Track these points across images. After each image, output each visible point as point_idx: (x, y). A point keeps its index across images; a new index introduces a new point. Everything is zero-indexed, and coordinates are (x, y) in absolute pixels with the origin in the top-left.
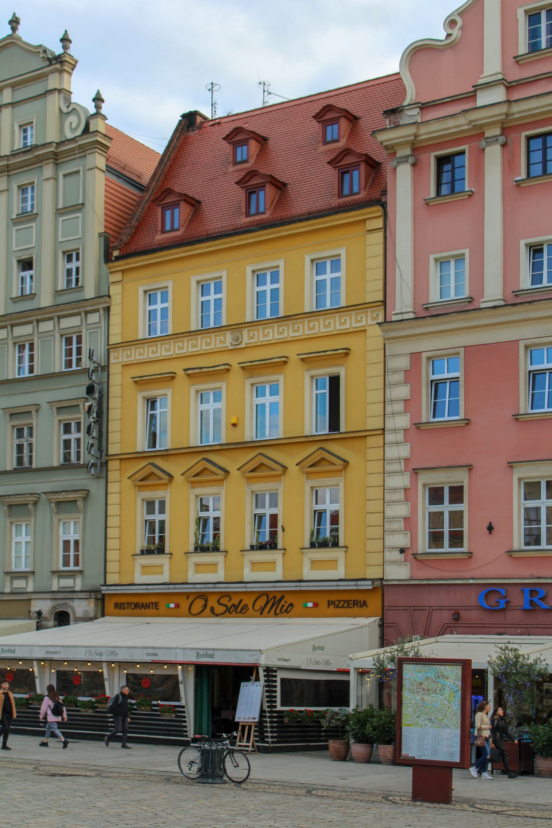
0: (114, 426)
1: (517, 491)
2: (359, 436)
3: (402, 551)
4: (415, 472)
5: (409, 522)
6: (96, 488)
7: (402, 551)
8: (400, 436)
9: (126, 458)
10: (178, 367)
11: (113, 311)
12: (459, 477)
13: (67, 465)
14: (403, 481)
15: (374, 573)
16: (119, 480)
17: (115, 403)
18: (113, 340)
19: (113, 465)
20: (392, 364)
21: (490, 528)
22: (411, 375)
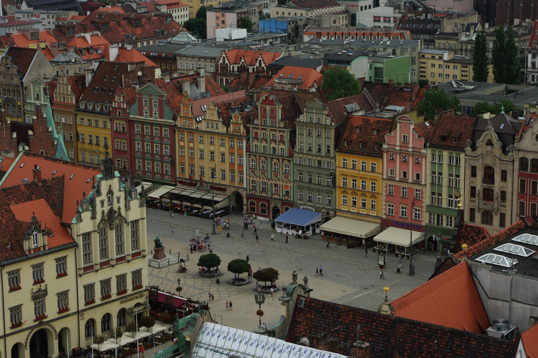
1: (401, 208)
2: (378, 194)
9: (340, 187)
10: (349, 174)
13: (328, 186)
14: (384, 203)
15: (380, 216)
16: (338, 191)
17: (337, 177)
19: (337, 188)
22: (386, 187)
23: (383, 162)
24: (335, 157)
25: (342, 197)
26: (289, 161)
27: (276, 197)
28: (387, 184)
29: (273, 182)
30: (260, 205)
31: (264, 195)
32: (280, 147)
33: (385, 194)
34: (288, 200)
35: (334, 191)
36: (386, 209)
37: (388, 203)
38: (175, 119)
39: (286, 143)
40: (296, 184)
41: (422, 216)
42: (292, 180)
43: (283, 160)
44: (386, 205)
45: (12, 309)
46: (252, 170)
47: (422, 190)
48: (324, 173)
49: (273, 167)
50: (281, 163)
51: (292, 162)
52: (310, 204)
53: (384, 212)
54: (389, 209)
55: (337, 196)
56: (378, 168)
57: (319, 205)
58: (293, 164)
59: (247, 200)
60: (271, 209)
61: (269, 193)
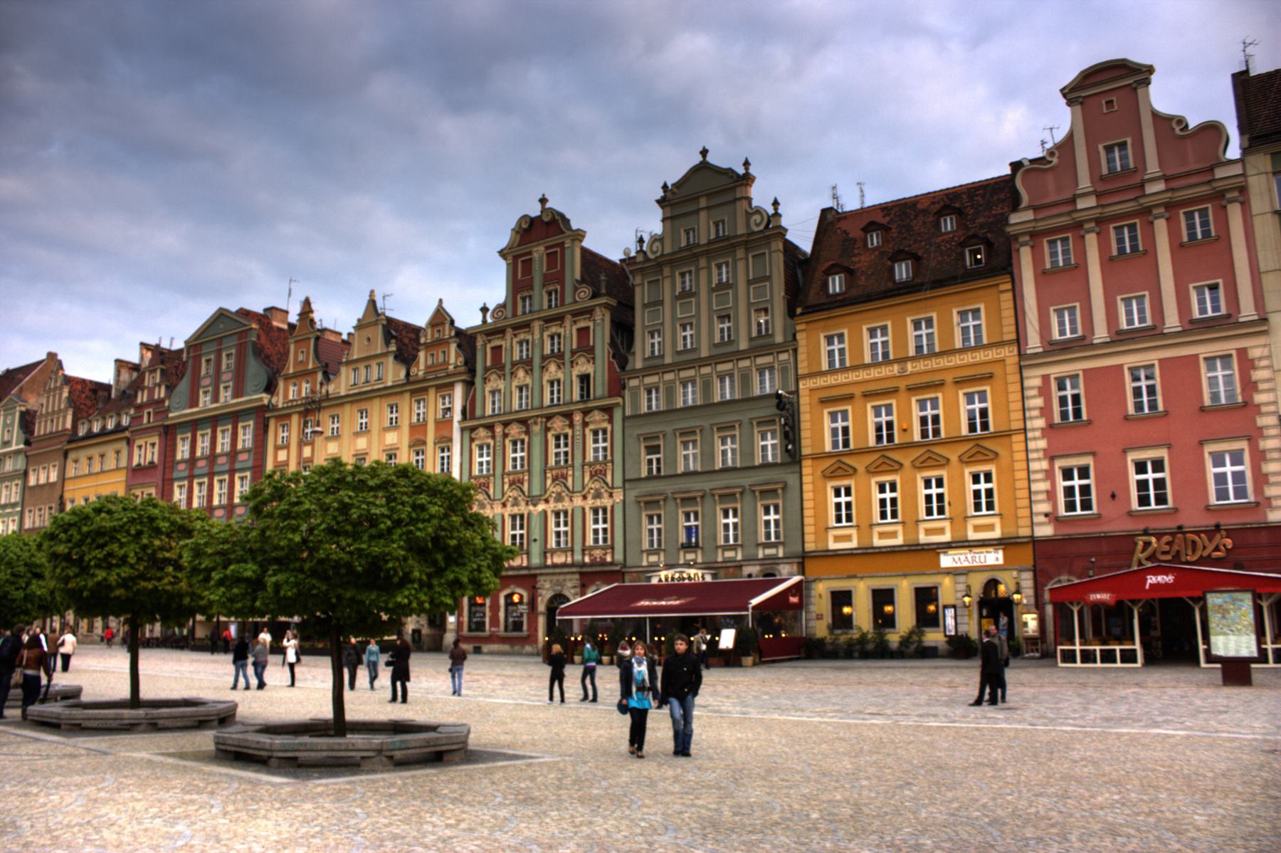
2: (1006, 435)
3: (1046, 515)
5: (1051, 495)
6: (792, 480)
7: (1046, 515)
8: (1038, 434)
10: (857, 391)
11: (800, 350)
14: (1044, 465)
17: (805, 418)
18: (800, 372)
20: (1027, 383)
21: (1113, 496)
26: (608, 410)
27: (559, 559)
32: (577, 371)
34: (603, 563)
35: (792, 480)
37: (1059, 464)
39: (598, 351)
40: (632, 495)
42: (618, 482)
44: (1049, 475)
47: (1242, 352)
48: (745, 417)
50: (578, 427)
51: (618, 415)
52: (690, 556)
54: (1069, 491)
55: (808, 495)
57: (730, 554)
58: (625, 418)
60: (541, 607)
61: (536, 549)
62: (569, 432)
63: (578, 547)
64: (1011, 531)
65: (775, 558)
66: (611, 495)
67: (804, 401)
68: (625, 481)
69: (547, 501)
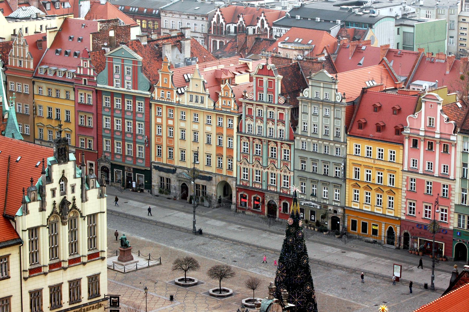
0: (347, 172)
1: (424, 207)
2: (397, 189)
4: (407, 199)
5: (406, 208)
12: (414, 202)
13: (336, 177)
14: (405, 200)
15: (399, 216)
19: (347, 181)
22: (407, 180)
23: (403, 149)
24: (345, 143)
25: (353, 191)
26: (289, 145)
27: (272, 189)
28: (408, 177)
29: (270, 171)
30: (252, 199)
31: (257, 186)
32: (279, 128)
33: (405, 189)
34: (287, 194)
36: (406, 208)
37: (408, 201)
38: (151, 89)
41: (450, 218)
42: (292, 169)
43: (282, 144)
44: (406, 203)
45: (31, 293)
46: (245, 155)
47: (450, 185)
48: (332, 161)
49: (270, 152)
50: (279, 147)
51: (292, 147)
52: (314, 199)
53: (404, 212)
56: (399, 158)
57: (325, 201)
59: (237, 192)
60: (266, 204)
61: (264, 184)
62: (276, 148)
63: (279, 187)
64: (396, 216)
65: (337, 206)
66: (290, 173)
67: (348, 162)
68: (294, 169)
69: (268, 169)
